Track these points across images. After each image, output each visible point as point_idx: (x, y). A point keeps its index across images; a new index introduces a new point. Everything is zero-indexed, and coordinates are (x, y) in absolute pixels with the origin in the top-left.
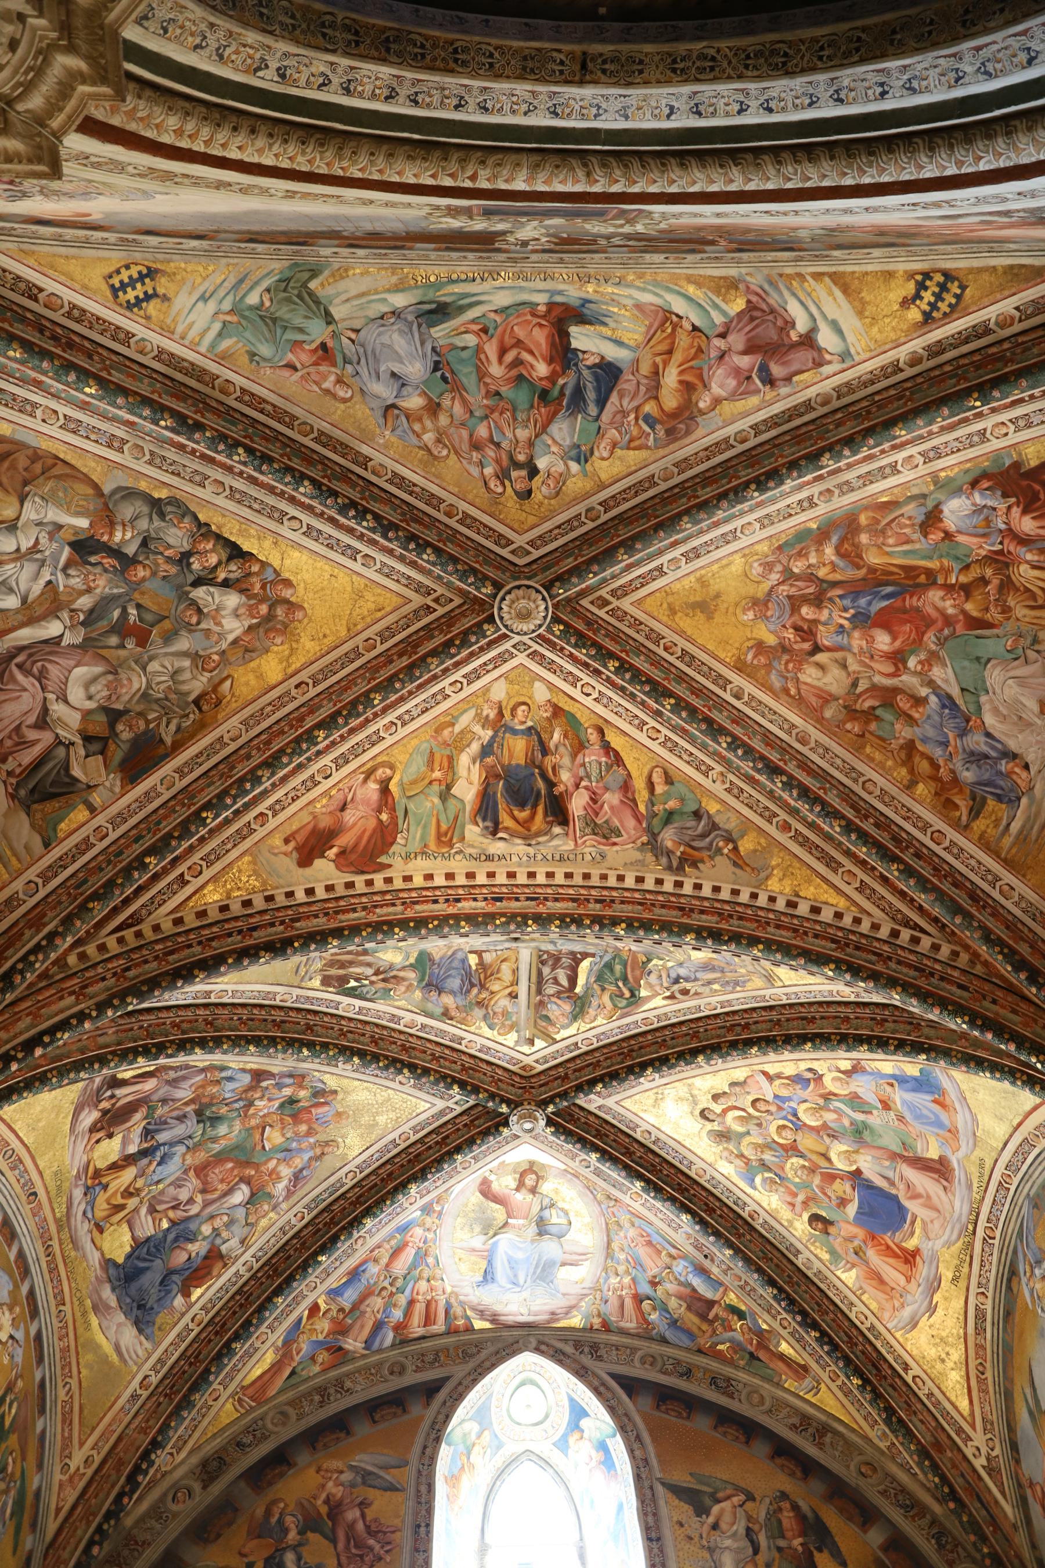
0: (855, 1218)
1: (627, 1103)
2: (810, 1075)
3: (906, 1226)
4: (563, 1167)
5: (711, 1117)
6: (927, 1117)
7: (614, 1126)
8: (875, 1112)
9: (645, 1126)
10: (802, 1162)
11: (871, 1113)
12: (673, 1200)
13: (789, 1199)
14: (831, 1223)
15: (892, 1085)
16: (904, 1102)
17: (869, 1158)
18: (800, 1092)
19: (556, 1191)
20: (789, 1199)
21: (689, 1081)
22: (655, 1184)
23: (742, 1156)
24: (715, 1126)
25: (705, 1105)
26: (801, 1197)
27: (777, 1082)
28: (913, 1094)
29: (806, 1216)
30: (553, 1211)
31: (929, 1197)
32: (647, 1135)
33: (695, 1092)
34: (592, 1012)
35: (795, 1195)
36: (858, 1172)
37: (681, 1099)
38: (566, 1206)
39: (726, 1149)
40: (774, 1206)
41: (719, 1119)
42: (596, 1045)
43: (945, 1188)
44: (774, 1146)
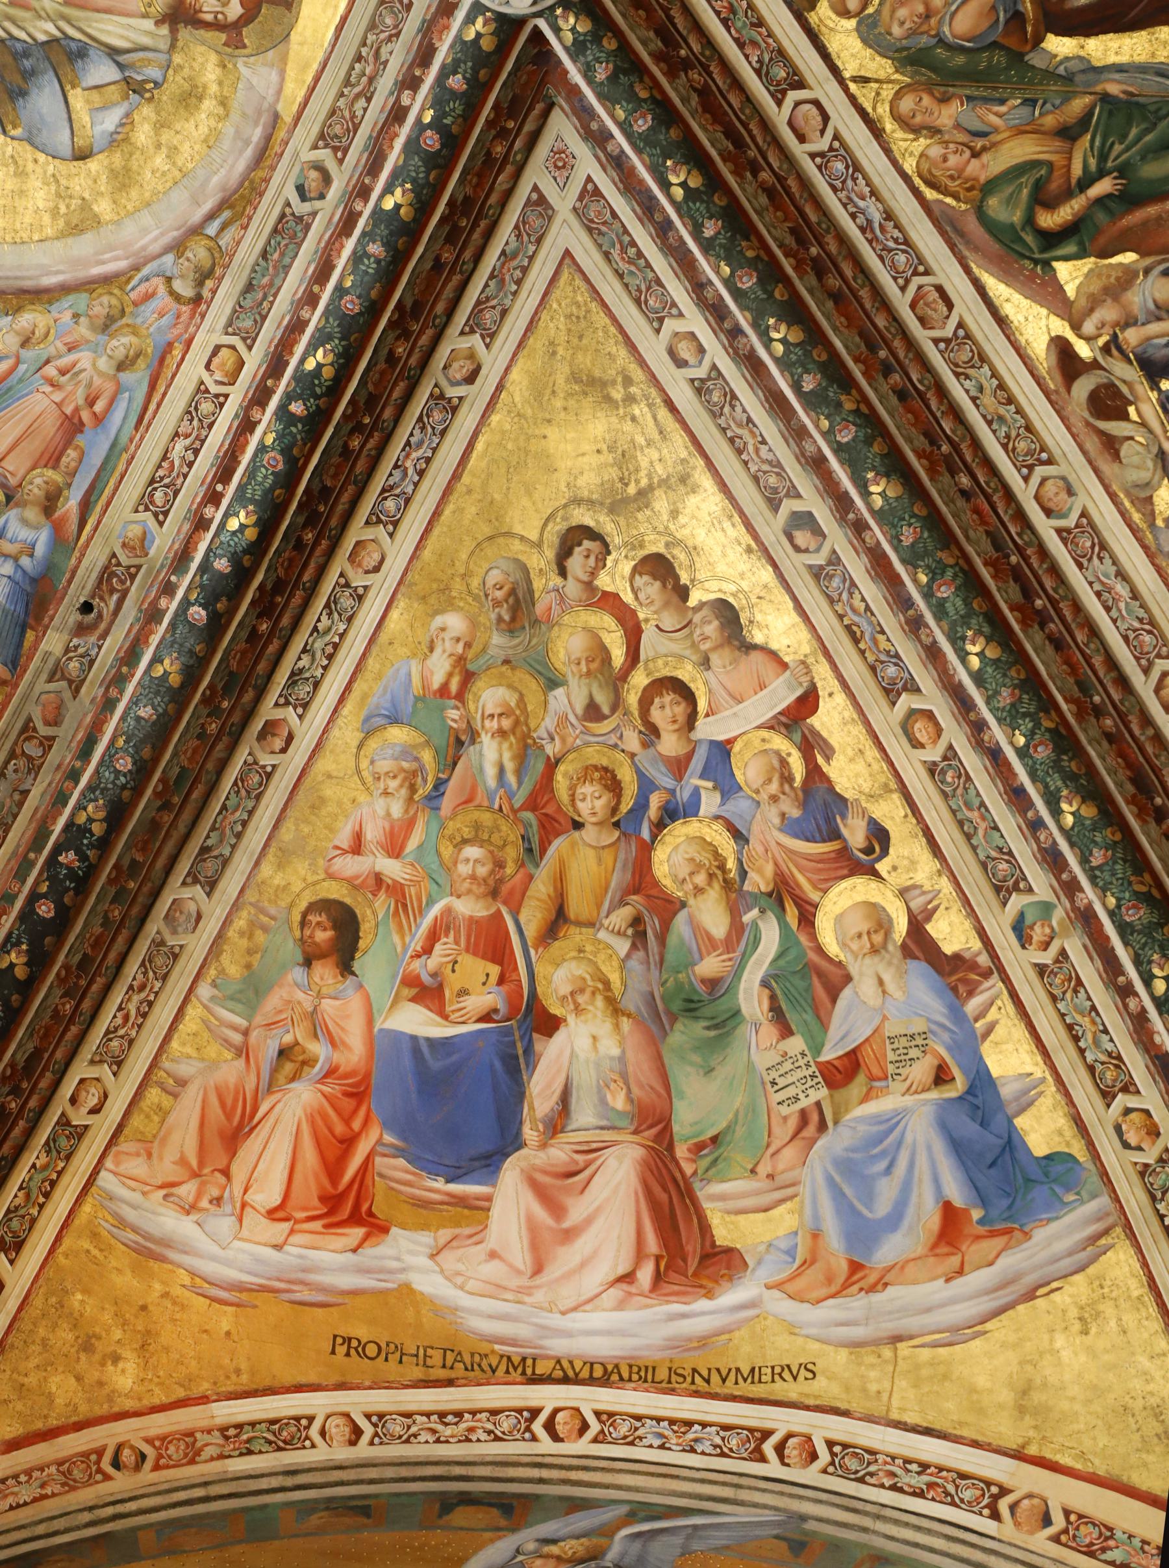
0: (396, 1037)
1: (568, 291)
2: (855, 834)
3: (440, 1184)
4: (287, 113)
5: (577, 563)
6: (869, 1198)
7: (478, 258)
8: (796, 1044)
9: (493, 361)
10: (511, 854)
11: (786, 1032)
12: (289, 479)
13: (372, 834)
14: (346, 967)
15: (941, 1077)
16: (891, 1124)
17: (610, 1047)
18: (772, 814)
19: (191, 98)
20: (372, 834)
21: (706, 482)
22: (328, 414)
23: (468, 677)
24: (545, 582)
25: (615, 540)
26: (392, 869)
27: (780, 743)
28: (940, 1147)
29: (335, 891)
30: (113, 92)
31: (568, 1235)
32: (460, 370)
33: (661, 503)
34: (948, 115)
35: (394, 849)
36: (550, 1025)
37: (624, 458)
38: (143, 134)
39: (474, 624)
40: (329, 791)
41: (572, 588)
42: (799, 151)
43: (628, 1278)
44: (540, 766)
